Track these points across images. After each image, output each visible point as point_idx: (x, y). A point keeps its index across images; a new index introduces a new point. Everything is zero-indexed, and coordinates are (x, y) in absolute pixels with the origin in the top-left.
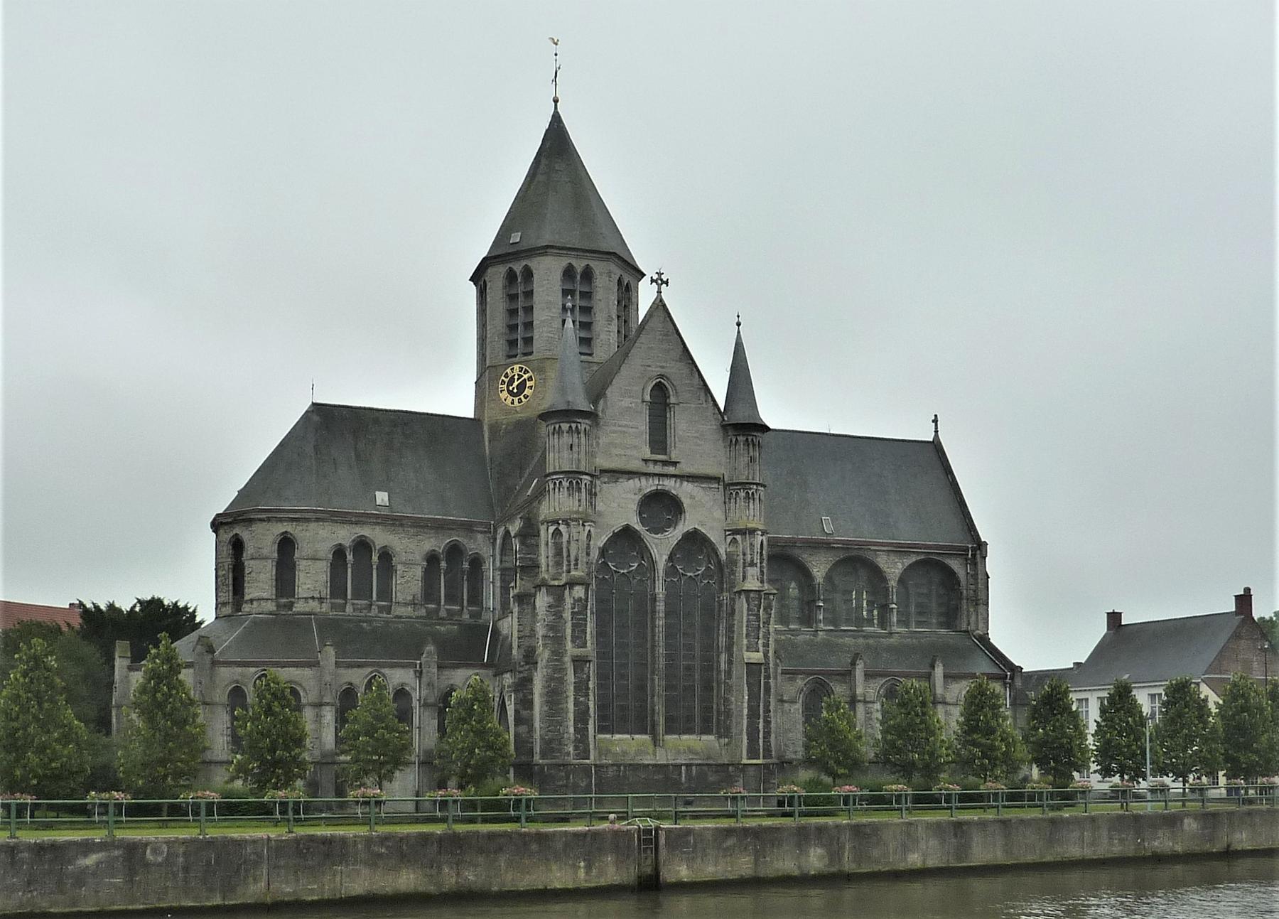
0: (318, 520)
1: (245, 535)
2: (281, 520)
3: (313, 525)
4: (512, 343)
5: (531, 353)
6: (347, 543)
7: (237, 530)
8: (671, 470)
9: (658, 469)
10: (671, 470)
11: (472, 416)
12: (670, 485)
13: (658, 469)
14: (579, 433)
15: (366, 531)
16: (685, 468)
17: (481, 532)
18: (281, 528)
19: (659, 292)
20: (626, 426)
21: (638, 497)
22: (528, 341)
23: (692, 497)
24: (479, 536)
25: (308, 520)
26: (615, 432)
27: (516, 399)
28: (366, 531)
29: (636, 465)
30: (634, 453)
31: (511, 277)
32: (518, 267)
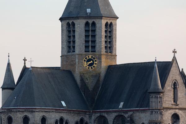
0: (52, 112)
1: (30, 115)
2: (42, 112)
3: (51, 113)
4: (87, 47)
5: (95, 51)
6: (58, 119)
7: (26, 114)
8: (177, 107)
9: (174, 107)
10: (177, 107)
11: (59, 65)
12: (177, 111)
13: (174, 107)
14: (158, 98)
15: (62, 115)
16: (180, 106)
17: (88, 114)
18: (42, 114)
19: (174, 55)
20: (169, 95)
21: (171, 115)
22: (93, 47)
23: (181, 115)
24: (87, 115)
25: (49, 112)
26: (167, 97)
27: (90, 67)
28: (62, 115)
29: (170, 106)
30: (170, 103)
31: (87, 24)
32: (90, 22)
